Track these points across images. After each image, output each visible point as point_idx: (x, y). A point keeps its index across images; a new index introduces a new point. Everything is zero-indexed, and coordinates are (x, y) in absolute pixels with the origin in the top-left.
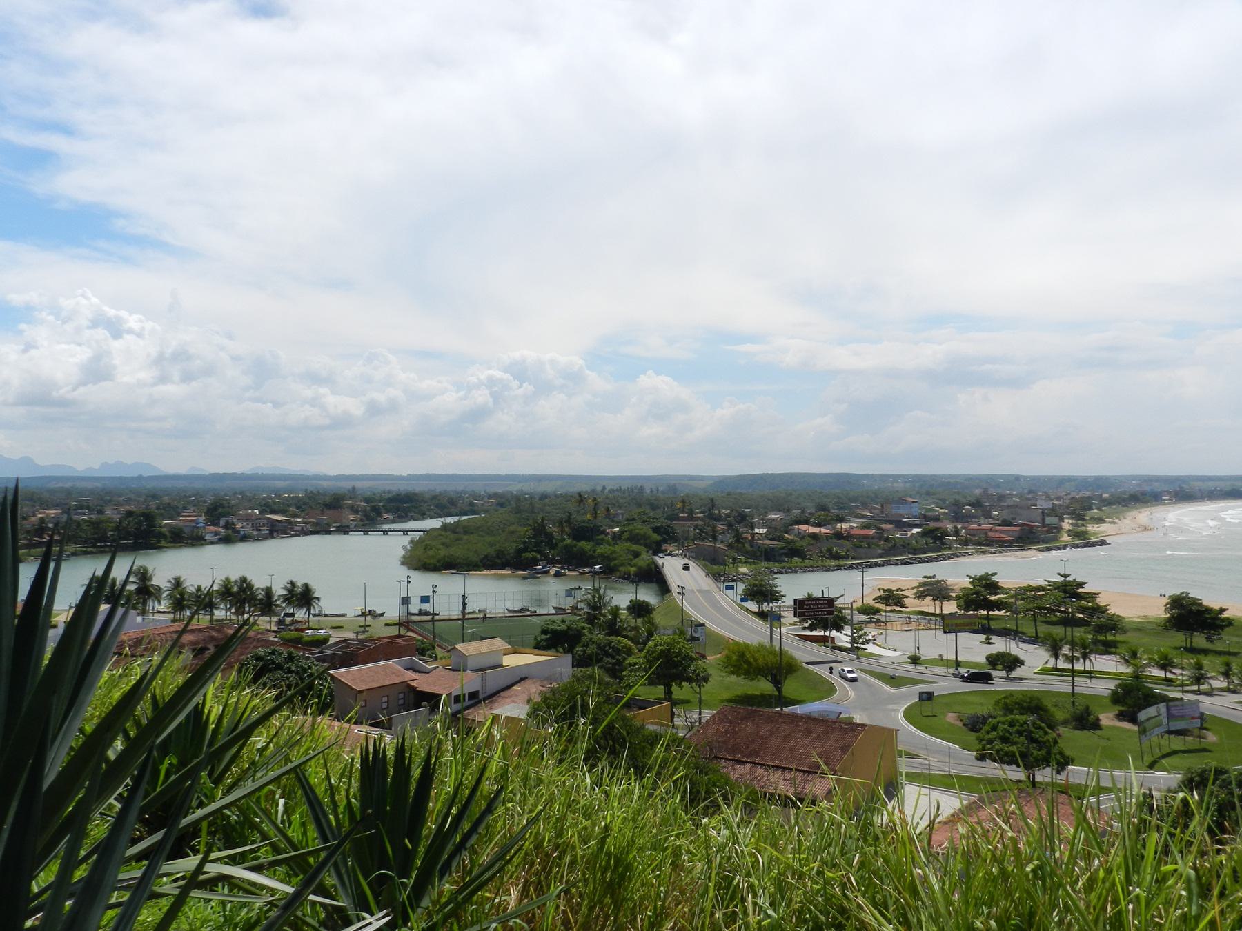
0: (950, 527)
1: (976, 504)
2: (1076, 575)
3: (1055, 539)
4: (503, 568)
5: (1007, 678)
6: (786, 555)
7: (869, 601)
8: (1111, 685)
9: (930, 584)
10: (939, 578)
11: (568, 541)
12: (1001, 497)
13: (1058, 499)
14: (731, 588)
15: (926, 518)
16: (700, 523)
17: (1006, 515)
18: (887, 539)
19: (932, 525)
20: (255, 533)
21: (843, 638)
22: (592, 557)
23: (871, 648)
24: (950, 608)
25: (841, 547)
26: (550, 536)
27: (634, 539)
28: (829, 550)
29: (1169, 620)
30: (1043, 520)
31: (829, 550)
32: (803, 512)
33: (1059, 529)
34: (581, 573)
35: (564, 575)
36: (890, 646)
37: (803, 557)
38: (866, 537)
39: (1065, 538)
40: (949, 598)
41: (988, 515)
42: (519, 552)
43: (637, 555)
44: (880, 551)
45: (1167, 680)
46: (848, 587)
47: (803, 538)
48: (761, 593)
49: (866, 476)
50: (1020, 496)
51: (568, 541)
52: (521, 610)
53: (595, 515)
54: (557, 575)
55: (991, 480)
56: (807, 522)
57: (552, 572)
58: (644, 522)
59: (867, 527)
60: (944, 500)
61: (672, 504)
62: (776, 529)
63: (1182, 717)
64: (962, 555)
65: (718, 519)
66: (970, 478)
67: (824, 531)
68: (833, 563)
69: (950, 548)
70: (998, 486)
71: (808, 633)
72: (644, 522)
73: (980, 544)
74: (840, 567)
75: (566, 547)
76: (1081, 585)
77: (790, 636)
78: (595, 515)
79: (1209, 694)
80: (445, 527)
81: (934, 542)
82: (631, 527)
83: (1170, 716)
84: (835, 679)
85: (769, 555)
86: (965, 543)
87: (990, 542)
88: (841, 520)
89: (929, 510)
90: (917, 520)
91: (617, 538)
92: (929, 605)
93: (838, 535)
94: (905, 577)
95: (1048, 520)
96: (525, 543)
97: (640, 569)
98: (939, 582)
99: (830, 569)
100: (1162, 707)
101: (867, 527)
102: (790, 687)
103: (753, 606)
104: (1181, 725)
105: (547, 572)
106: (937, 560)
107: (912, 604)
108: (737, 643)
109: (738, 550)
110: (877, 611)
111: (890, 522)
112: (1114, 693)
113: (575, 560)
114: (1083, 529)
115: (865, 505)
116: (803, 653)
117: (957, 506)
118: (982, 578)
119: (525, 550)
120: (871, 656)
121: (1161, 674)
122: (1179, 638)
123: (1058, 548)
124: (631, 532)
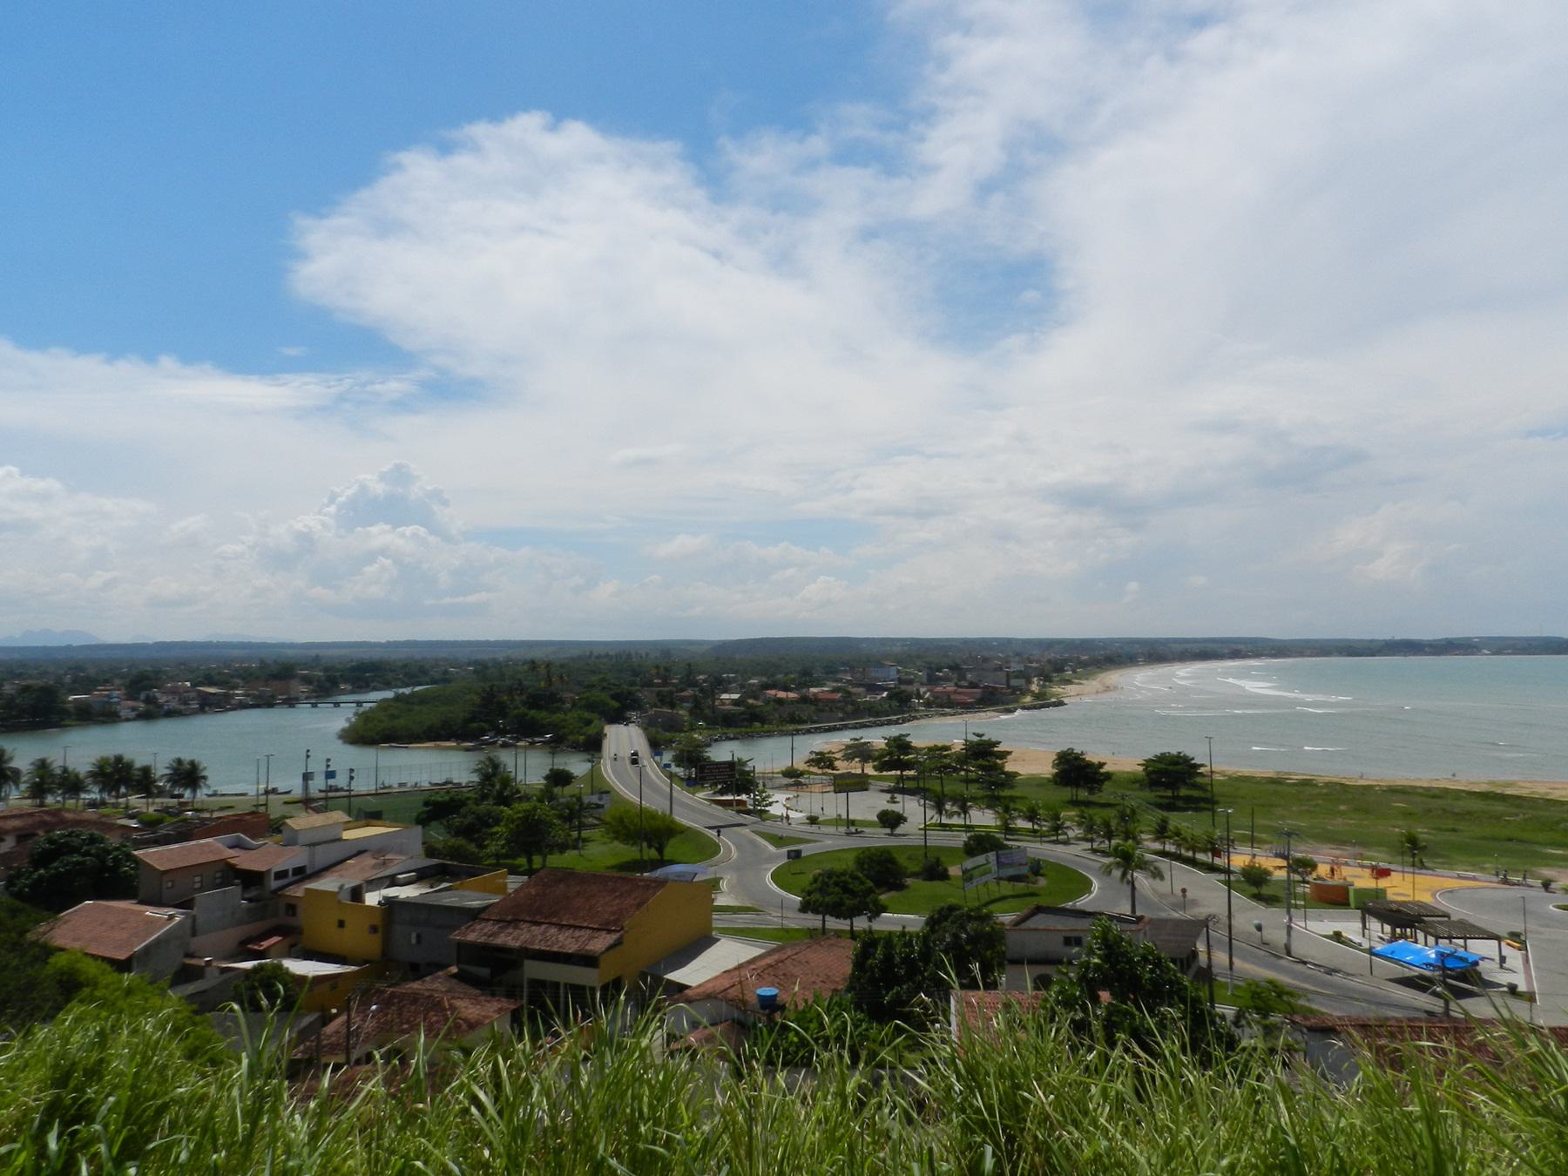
2: (991, 735)
5: (891, 835)
7: (800, 765)
8: (964, 837)
18: (853, 703)
29: (1056, 775)
37: (763, 721)
38: (833, 701)
45: (1035, 831)
63: (1011, 865)
67: (792, 695)
68: (791, 727)
73: (941, 706)
79: (1066, 843)
80: (398, 698)
83: (999, 864)
86: (928, 704)
87: (951, 704)
93: (804, 700)
100: (992, 856)
104: (1011, 872)
112: (966, 844)
121: (1029, 825)
122: (1067, 793)
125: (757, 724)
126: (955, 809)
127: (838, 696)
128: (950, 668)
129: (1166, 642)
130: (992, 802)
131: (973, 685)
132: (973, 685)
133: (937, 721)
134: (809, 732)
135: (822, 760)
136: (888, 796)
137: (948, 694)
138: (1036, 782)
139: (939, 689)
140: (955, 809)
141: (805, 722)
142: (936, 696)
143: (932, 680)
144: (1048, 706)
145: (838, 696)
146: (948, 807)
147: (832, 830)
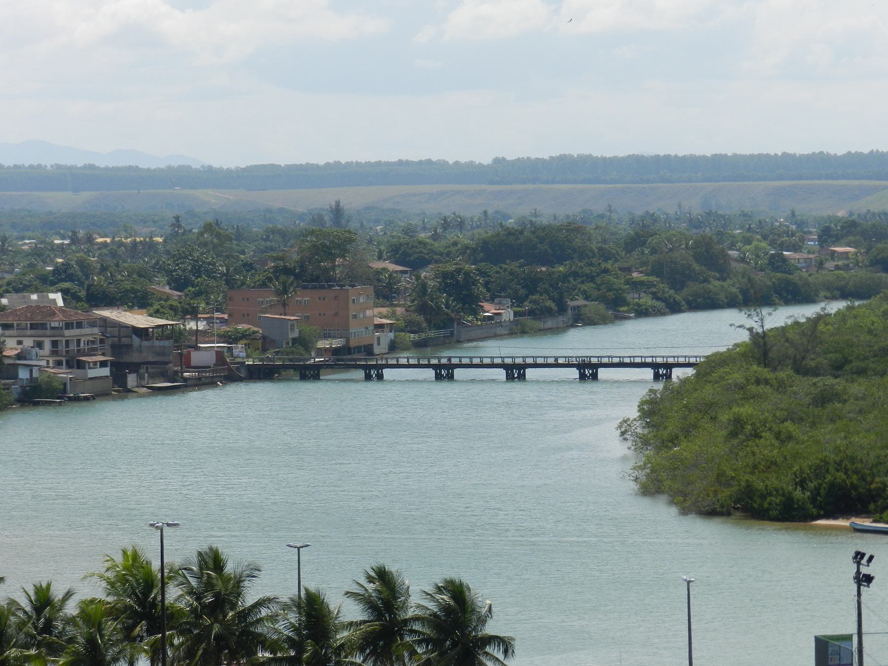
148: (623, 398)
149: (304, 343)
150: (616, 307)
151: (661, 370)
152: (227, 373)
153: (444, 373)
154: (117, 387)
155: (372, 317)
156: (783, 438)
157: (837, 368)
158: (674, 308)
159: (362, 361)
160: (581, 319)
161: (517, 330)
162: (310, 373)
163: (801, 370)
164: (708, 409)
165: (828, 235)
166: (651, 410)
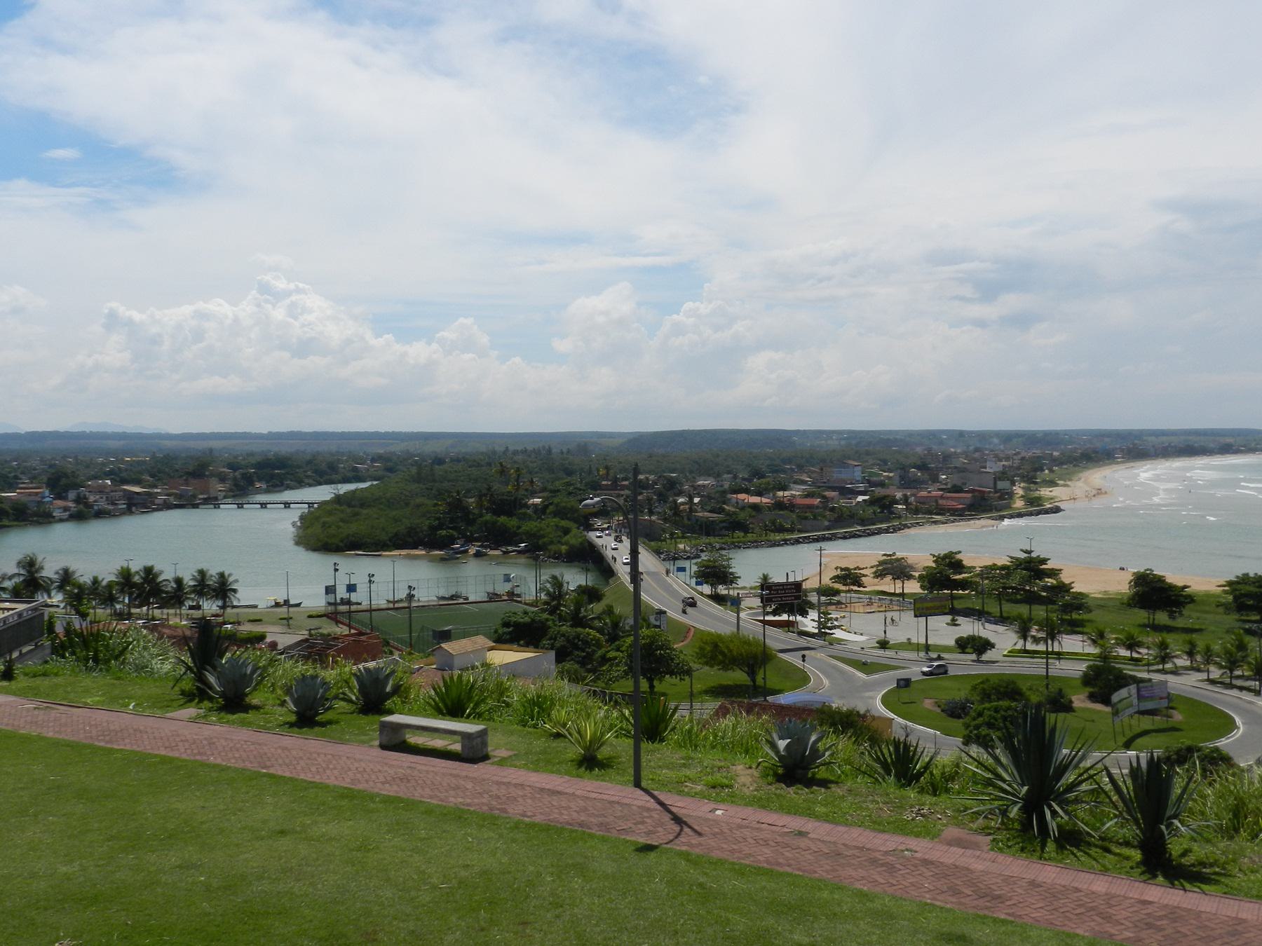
0: (899, 495)
1: (922, 467)
3: (1009, 507)
4: (416, 548)
6: (727, 529)
8: (1083, 667)
9: (890, 562)
10: (899, 555)
11: (488, 517)
12: (947, 457)
13: (1007, 459)
14: (682, 569)
15: (872, 484)
16: (627, 492)
17: (955, 479)
18: (833, 509)
19: (880, 492)
20: (111, 507)
21: (809, 623)
22: (516, 534)
23: (838, 634)
24: (913, 587)
25: (787, 519)
26: (466, 511)
27: (561, 513)
28: (773, 523)
30: (995, 483)
31: (773, 523)
32: (735, 477)
33: (1011, 495)
34: (505, 553)
35: (485, 554)
36: (858, 630)
38: (810, 507)
39: (1019, 504)
40: (910, 577)
41: (935, 479)
42: (433, 529)
43: (566, 531)
44: (826, 523)
45: (1132, 659)
46: (804, 563)
47: (743, 508)
48: (716, 575)
49: (797, 432)
50: (966, 454)
51: (488, 517)
52: (452, 598)
53: (518, 488)
54: (478, 555)
55: (932, 435)
56: (747, 491)
57: (472, 551)
58: (570, 494)
59: (809, 495)
60: (885, 462)
61: (590, 472)
62: (710, 498)
64: (913, 525)
65: (644, 486)
66: (911, 434)
67: (765, 500)
69: (900, 517)
70: (941, 443)
71: (768, 618)
72: (570, 494)
74: (786, 542)
75: (486, 522)
76: (1044, 561)
77: (748, 618)
78: (518, 488)
81: (881, 514)
82: (556, 500)
84: (809, 667)
85: (707, 529)
88: (784, 489)
89: (871, 474)
90: (861, 487)
91: (541, 511)
92: (888, 585)
94: (862, 552)
95: (1001, 485)
96: (439, 519)
97: (572, 547)
98: (898, 560)
99: (775, 544)
101: (809, 495)
102: (768, 677)
103: (707, 589)
105: (466, 551)
106: (887, 531)
107: (871, 584)
108: (709, 634)
109: (676, 524)
110: (837, 592)
111: (833, 489)
113: (499, 538)
114: (1037, 494)
115: (801, 468)
116: (777, 639)
117: (904, 468)
118: (946, 556)
119: (440, 527)
120: (839, 641)
123: (1011, 517)
124: (557, 505)
125: (739, 534)
126: (1042, 635)
127: (817, 501)
128: (918, 468)
129: (1140, 434)
130: (1074, 627)
131: (957, 489)
132: (957, 489)
133: (941, 529)
134: (797, 542)
135: (850, 577)
136: (948, 618)
137: (936, 499)
138: (1105, 604)
139: (924, 493)
140: (1042, 635)
141: (791, 531)
142: (922, 501)
143: (906, 482)
144: (1038, 513)
145: (817, 501)
146: (1033, 633)
147: (912, 655)
148: (294, 515)
149: (194, 496)
150: (300, 484)
151: (310, 504)
152: (167, 506)
153: (240, 506)
154: (129, 511)
155: (218, 487)
156: (339, 527)
157: (362, 505)
158: (320, 484)
159: (212, 501)
160: (290, 488)
161: (267, 491)
162: (195, 506)
163: (349, 506)
164: (317, 518)
165: (373, 460)
166: (302, 518)
